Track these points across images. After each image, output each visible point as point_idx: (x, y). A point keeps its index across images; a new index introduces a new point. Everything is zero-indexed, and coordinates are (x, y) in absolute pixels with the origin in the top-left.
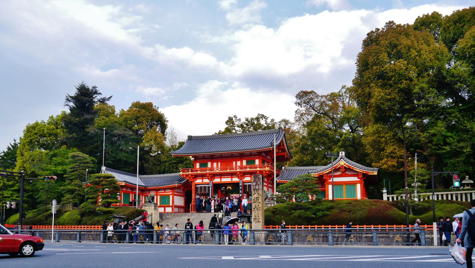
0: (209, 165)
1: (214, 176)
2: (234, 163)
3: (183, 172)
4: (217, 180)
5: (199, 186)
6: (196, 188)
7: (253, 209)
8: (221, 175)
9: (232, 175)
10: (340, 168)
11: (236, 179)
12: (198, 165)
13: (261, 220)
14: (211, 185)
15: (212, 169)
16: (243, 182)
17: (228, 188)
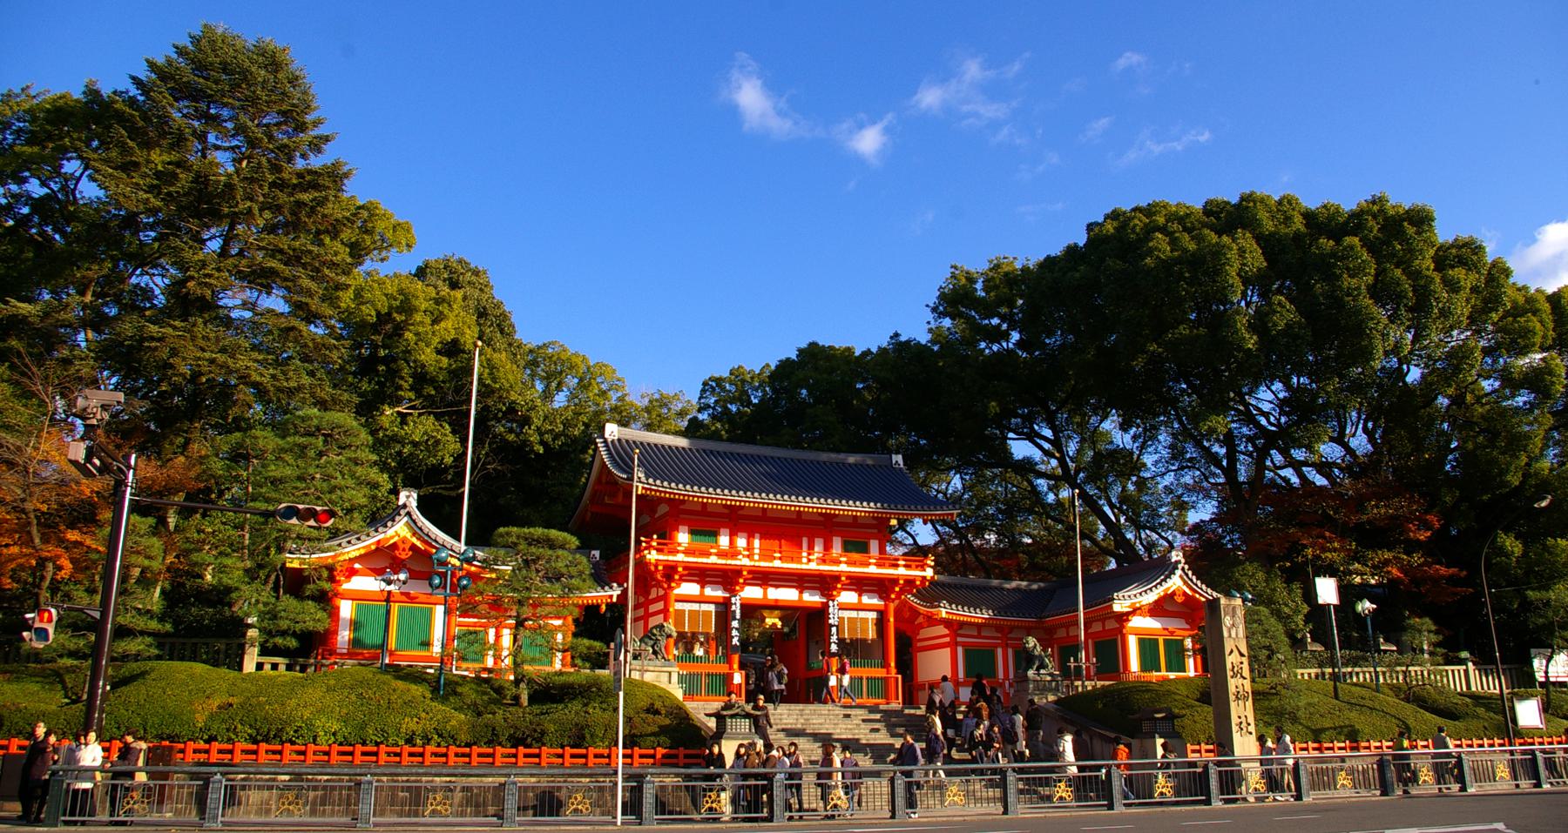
0: (724, 541)
1: (729, 578)
2: (805, 541)
3: (659, 551)
4: (753, 593)
5: (687, 607)
6: (680, 613)
7: (1232, 697)
8: (764, 578)
9: (801, 581)
10: (1174, 593)
11: (812, 598)
12: (683, 537)
13: (1252, 728)
14: (737, 609)
15: (733, 552)
16: (842, 607)
17: (769, 621)
